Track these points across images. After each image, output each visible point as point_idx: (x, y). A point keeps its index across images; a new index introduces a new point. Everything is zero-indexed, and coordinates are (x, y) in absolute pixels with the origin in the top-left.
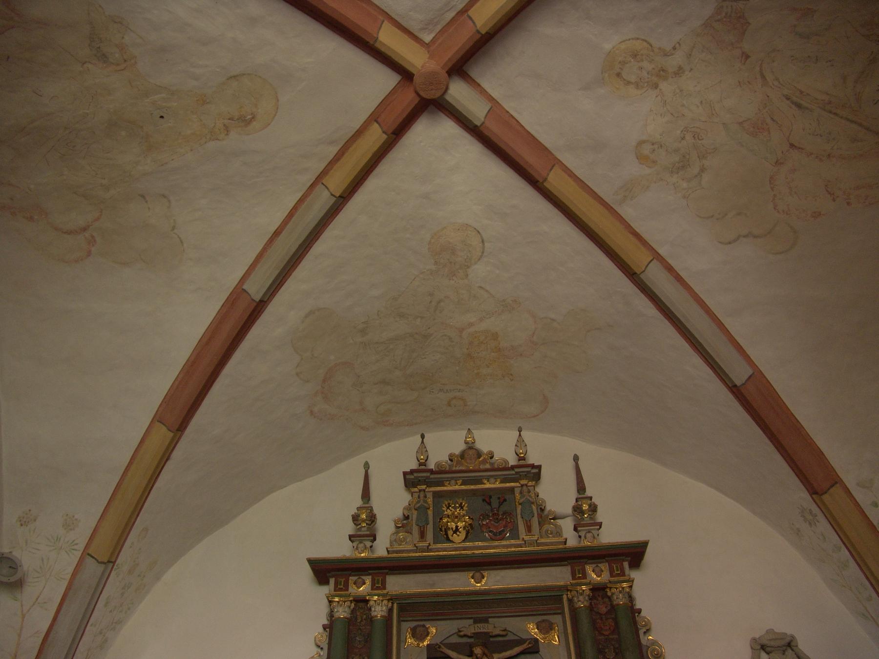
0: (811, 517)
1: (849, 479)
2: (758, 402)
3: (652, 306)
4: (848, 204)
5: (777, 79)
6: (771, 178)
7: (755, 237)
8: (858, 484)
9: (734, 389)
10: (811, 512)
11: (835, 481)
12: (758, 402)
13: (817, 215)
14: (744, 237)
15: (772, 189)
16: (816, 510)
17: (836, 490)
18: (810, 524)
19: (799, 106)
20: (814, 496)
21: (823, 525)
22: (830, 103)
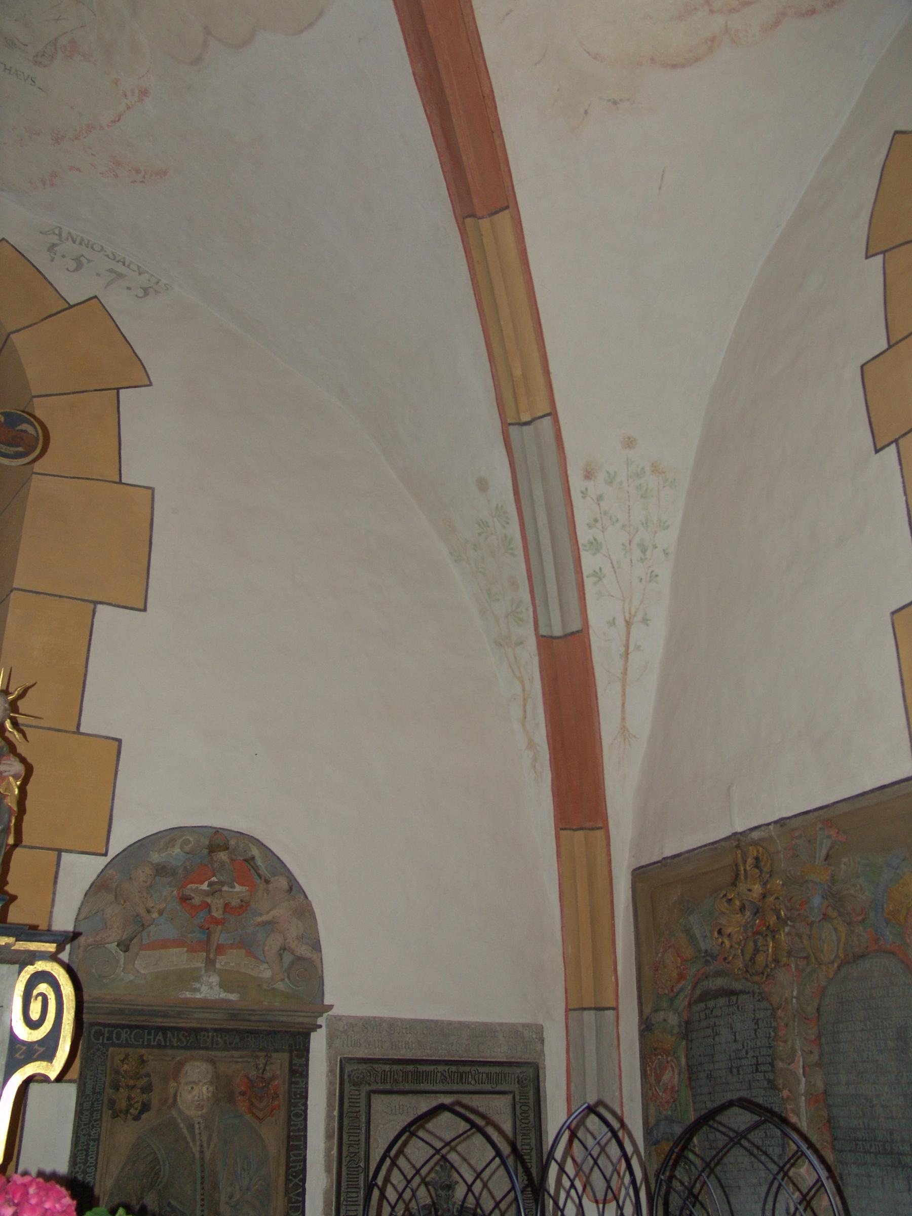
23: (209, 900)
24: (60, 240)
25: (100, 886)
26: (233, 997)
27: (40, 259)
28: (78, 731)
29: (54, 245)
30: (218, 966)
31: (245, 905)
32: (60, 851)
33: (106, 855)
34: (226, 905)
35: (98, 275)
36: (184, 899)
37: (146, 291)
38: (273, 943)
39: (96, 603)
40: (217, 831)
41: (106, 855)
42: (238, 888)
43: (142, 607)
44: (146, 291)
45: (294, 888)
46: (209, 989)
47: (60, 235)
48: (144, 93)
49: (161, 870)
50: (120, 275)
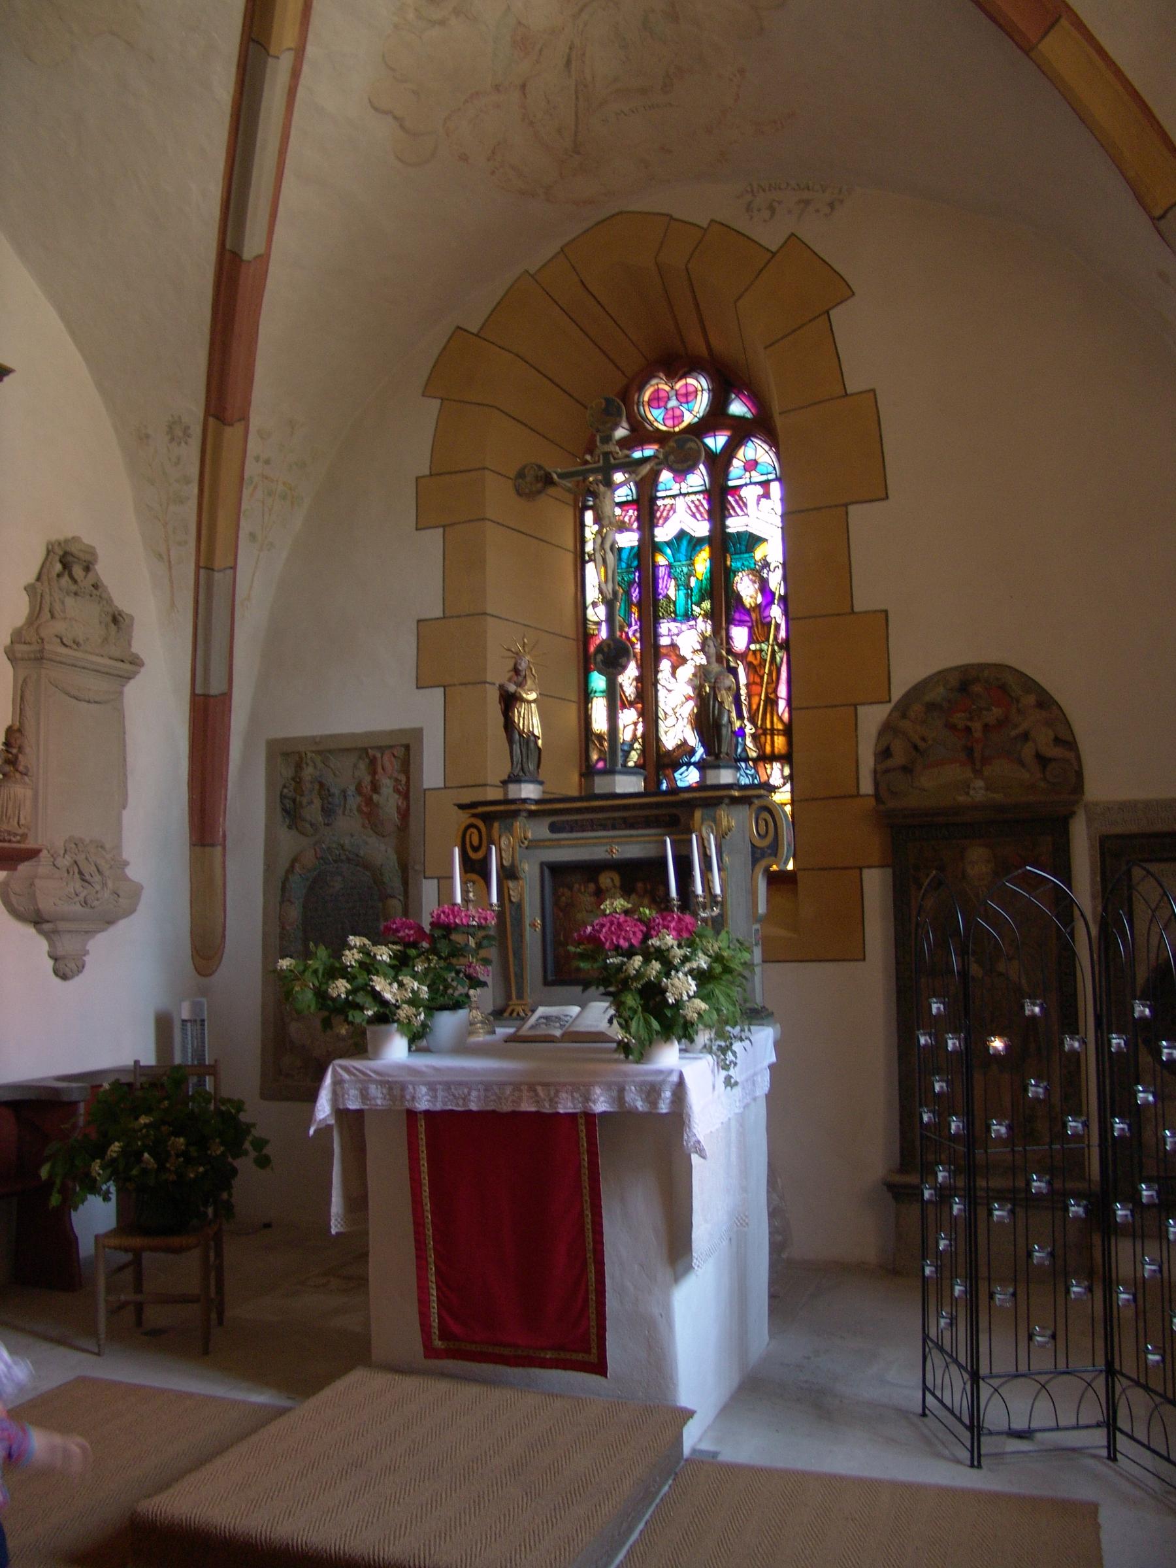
0: (180, 434)
1: (255, 421)
2: (233, 284)
3: (232, 90)
4: (493, 173)
5: (585, 25)
6: (477, 93)
7: (402, 127)
8: (259, 431)
9: (228, 256)
10: (186, 429)
11: (244, 418)
12: (233, 284)
13: (464, 158)
14: (395, 118)
15: (467, 101)
16: (197, 430)
17: (239, 427)
18: (172, 440)
19: (568, 63)
20: (211, 419)
21: (191, 452)
22: (585, 86)
23: (969, 724)
24: (754, 195)
25: (888, 728)
26: (998, 797)
27: (741, 225)
28: (853, 612)
29: (750, 203)
30: (986, 773)
31: (1002, 723)
32: (855, 706)
33: (890, 701)
34: (986, 727)
35: (790, 212)
36: (952, 727)
37: (831, 206)
38: (1028, 752)
39: (846, 505)
40: (965, 669)
41: (890, 701)
42: (995, 710)
43: (883, 496)
44: (831, 206)
45: (1045, 701)
46: (979, 792)
47: (752, 191)
48: (742, 71)
49: (931, 707)
50: (807, 202)
